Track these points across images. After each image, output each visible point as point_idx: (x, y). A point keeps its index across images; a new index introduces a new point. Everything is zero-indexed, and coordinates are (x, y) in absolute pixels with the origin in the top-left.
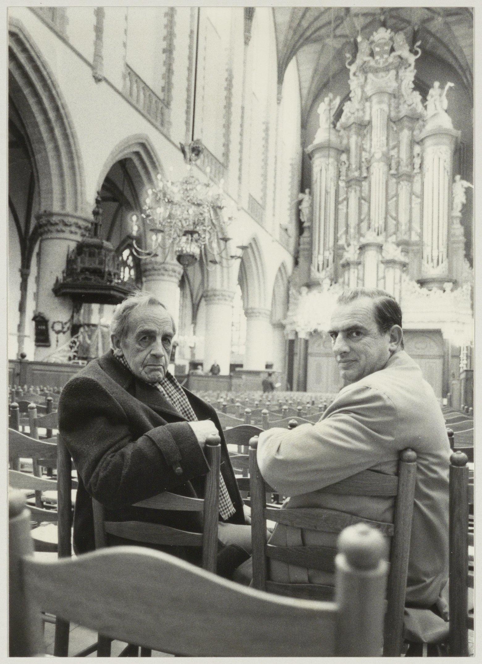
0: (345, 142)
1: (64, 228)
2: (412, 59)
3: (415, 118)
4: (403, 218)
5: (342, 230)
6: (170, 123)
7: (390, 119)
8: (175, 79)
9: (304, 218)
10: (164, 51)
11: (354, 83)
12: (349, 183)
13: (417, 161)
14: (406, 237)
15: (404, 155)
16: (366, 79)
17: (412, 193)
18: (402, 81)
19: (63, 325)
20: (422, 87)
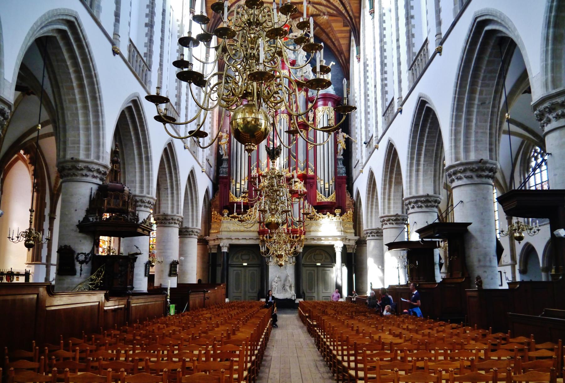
1: (88, 173)
5: (254, 164)
6: (150, 81)
9: (222, 152)
10: (146, 25)
13: (311, 115)
14: (304, 172)
18: (298, 55)
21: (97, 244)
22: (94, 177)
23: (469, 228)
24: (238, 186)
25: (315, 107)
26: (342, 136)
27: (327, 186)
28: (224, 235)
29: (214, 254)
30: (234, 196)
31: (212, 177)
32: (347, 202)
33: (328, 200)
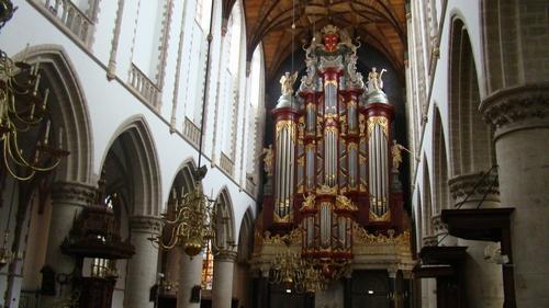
0: (302, 107)
2: (355, 49)
3: (359, 92)
4: (352, 173)
5: (300, 181)
6: (160, 102)
7: (339, 92)
8: (167, 69)
9: (267, 169)
11: (309, 62)
12: (307, 141)
14: (354, 189)
15: (351, 122)
16: (319, 60)
17: (359, 153)
19: (67, 276)
20: (364, 70)
21: (80, 266)
22: (79, 199)
23: (468, 250)
24: (282, 205)
25: (367, 118)
26: (397, 148)
27: (380, 203)
28: (264, 257)
29: (255, 279)
30: (277, 216)
31: (255, 196)
32: (404, 222)
33: (382, 219)
